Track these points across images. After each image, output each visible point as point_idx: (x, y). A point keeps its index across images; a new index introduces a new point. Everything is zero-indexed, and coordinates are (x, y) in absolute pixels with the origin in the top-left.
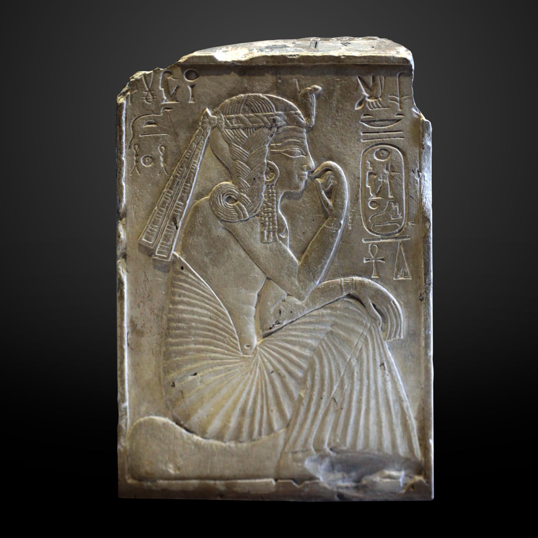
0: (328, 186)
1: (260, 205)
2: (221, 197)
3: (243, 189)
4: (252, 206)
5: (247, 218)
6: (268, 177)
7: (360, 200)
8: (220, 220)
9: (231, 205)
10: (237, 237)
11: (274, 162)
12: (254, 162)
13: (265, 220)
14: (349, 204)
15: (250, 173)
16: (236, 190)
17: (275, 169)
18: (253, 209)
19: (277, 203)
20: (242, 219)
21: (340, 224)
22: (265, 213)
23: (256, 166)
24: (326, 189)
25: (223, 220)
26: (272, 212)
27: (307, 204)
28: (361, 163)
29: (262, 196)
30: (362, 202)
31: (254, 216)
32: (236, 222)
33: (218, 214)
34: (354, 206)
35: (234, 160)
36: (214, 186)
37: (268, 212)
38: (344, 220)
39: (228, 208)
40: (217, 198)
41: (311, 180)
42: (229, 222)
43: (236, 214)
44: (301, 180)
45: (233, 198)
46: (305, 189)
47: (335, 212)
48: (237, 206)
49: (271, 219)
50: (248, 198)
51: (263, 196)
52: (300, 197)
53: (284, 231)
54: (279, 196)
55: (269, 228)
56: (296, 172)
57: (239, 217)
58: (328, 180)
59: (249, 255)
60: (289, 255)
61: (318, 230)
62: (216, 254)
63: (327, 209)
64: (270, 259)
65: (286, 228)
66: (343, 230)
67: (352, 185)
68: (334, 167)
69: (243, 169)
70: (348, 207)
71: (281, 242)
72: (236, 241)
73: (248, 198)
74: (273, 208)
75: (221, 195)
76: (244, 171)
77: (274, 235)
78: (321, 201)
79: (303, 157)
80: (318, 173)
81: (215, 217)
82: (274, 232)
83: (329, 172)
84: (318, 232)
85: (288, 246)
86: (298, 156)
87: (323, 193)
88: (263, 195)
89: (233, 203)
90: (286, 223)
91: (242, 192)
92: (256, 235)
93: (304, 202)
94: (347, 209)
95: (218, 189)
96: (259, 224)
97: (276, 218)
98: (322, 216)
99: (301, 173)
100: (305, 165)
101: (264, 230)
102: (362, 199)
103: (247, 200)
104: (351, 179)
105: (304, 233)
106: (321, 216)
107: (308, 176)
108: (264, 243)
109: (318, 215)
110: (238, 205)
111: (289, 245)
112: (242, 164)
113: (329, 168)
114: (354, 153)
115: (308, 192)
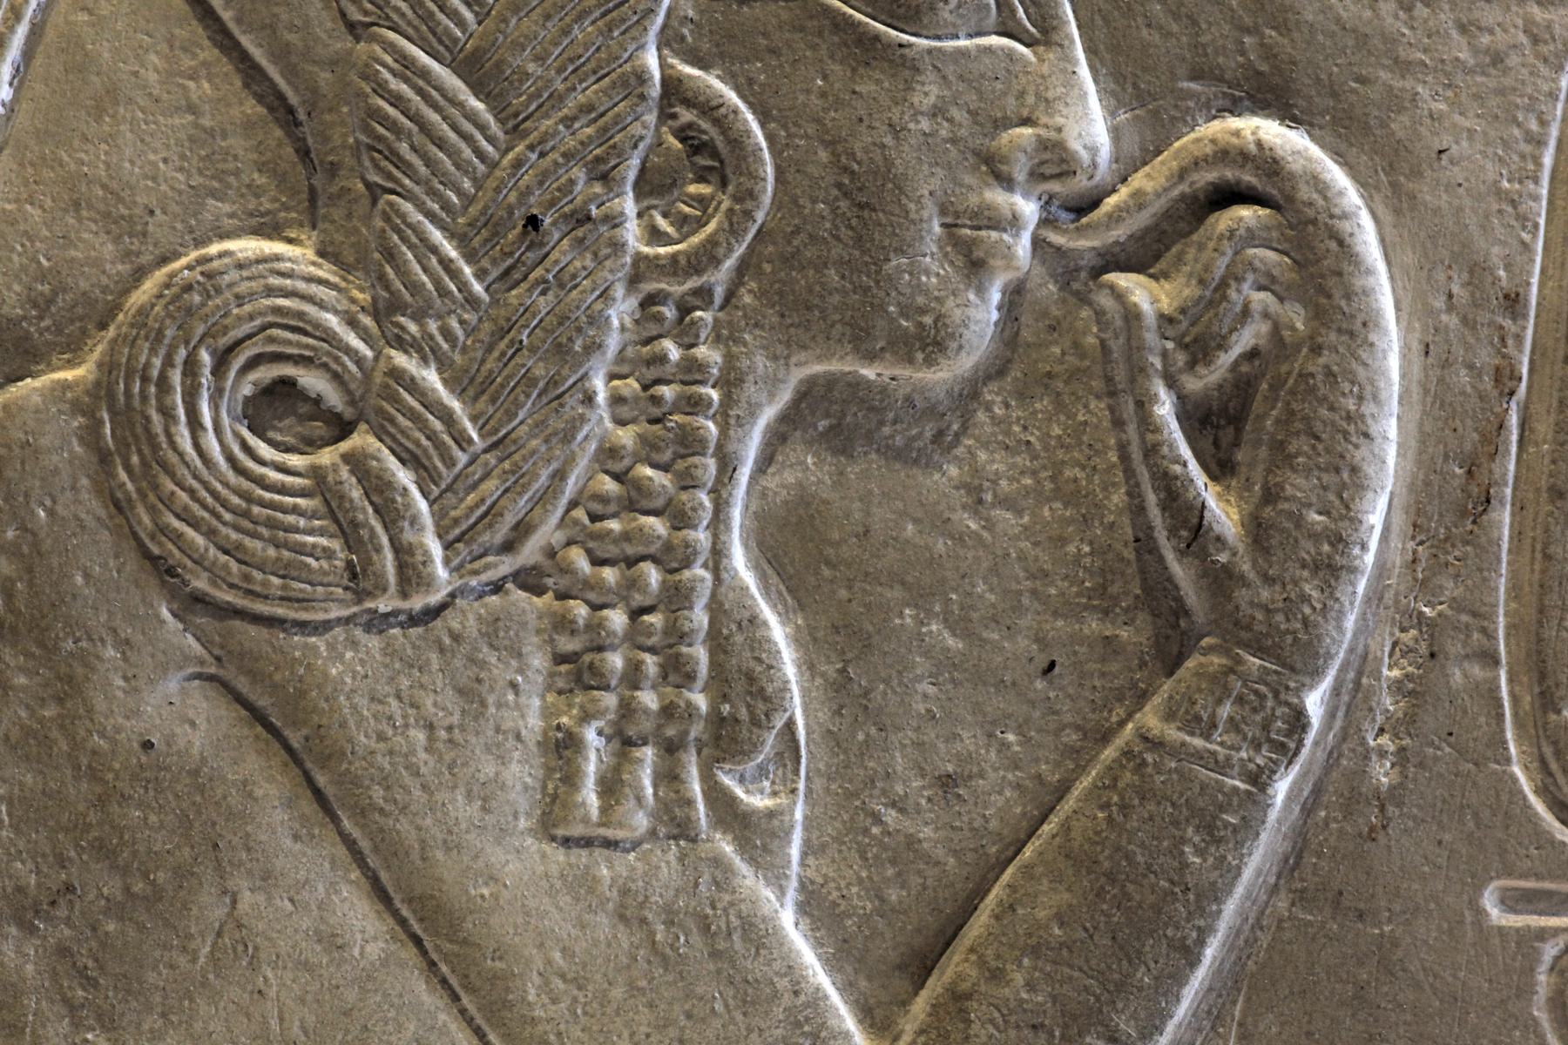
0: (1223, 346)
1: (560, 476)
2: (206, 378)
3: (418, 317)
4: (491, 486)
5: (435, 599)
6: (662, 224)
7: (1505, 516)
8: (173, 594)
9: (295, 460)
10: (325, 761)
11: (730, 78)
12: (540, 59)
13: (595, 627)
14: (1395, 542)
15: (494, 165)
16: (352, 323)
17: (738, 142)
18: (492, 514)
19: (727, 467)
20: (383, 605)
21: (1299, 720)
22: (598, 562)
23: (558, 99)
24: (1193, 384)
25: (199, 599)
26: (673, 558)
27: (997, 513)
28: (1548, 160)
29: (589, 399)
30: (1518, 535)
31: (497, 587)
32: (324, 627)
33: (164, 530)
34: (1438, 566)
35: (351, 27)
36: (140, 274)
37: (630, 550)
38: (1336, 691)
39: (260, 482)
40: (163, 384)
41: (1065, 286)
42: (257, 619)
43: (336, 545)
44: (975, 266)
45: (318, 401)
46: (995, 370)
47: (1265, 594)
48: (344, 472)
49: (655, 619)
50: (456, 405)
51: (601, 397)
52: (939, 435)
53: (770, 739)
54: (753, 411)
55: (627, 710)
56: (927, 184)
57: (359, 579)
58: (1223, 285)
59: (418, 942)
60: (792, 970)
61: (1081, 769)
62: (114, 909)
63: (1180, 571)
64: (617, 993)
65: (790, 725)
66: (1317, 791)
67: (1446, 364)
68: (1296, 166)
69: (435, 117)
70: (1381, 567)
71: (728, 849)
72: (308, 806)
73: (456, 405)
74: (681, 519)
75: (205, 357)
76: (441, 144)
77: (669, 777)
78: (1134, 493)
79: (1010, 55)
80: (1142, 220)
81: (132, 563)
82: (671, 749)
83: (1246, 213)
84: (1085, 782)
85: (791, 895)
86: (963, 43)
87: (1165, 409)
88: (599, 384)
89: (309, 445)
90: (790, 670)
91: (401, 343)
92: (503, 760)
93: (974, 493)
94: (1376, 596)
95: (178, 296)
96: (539, 661)
97: (700, 617)
98: (1133, 634)
99: (973, 200)
100: (1027, 131)
101: (586, 717)
102: (1519, 507)
103: (448, 418)
104: (1439, 303)
105: (946, 782)
106: (1124, 634)
107: (1038, 243)
108: (567, 842)
109: (1093, 625)
110: (355, 461)
111: (802, 886)
112: (425, 74)
113: (1249, 178)
114: (1497, 59)
115: (1023, 395)
